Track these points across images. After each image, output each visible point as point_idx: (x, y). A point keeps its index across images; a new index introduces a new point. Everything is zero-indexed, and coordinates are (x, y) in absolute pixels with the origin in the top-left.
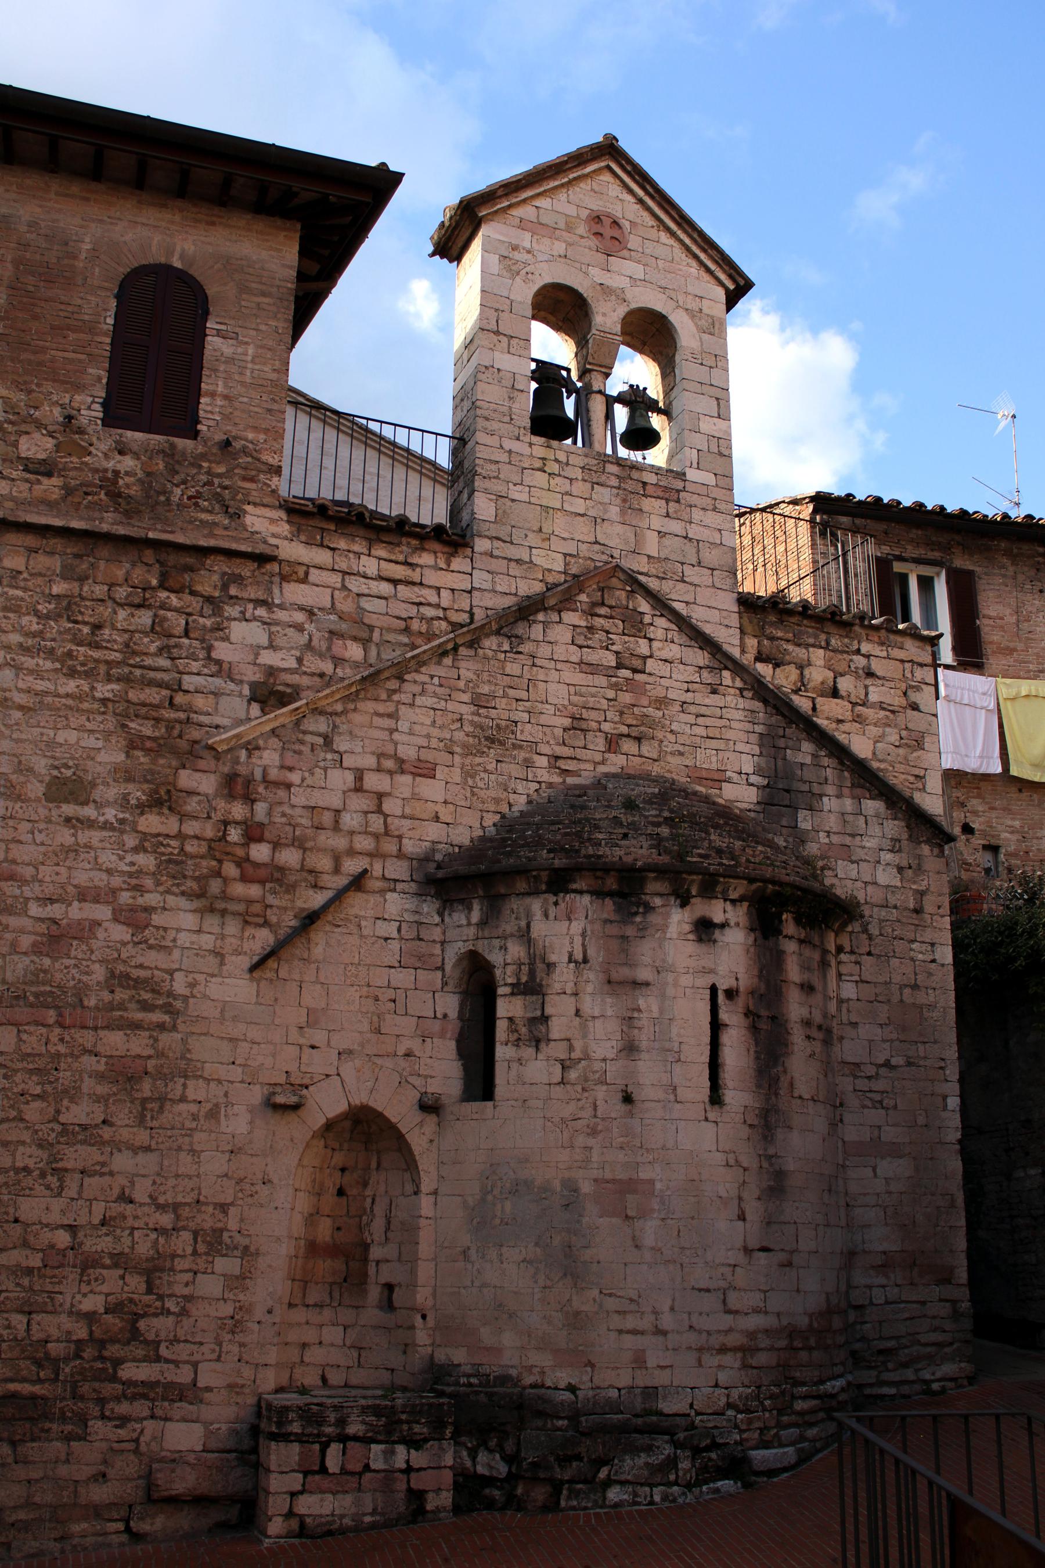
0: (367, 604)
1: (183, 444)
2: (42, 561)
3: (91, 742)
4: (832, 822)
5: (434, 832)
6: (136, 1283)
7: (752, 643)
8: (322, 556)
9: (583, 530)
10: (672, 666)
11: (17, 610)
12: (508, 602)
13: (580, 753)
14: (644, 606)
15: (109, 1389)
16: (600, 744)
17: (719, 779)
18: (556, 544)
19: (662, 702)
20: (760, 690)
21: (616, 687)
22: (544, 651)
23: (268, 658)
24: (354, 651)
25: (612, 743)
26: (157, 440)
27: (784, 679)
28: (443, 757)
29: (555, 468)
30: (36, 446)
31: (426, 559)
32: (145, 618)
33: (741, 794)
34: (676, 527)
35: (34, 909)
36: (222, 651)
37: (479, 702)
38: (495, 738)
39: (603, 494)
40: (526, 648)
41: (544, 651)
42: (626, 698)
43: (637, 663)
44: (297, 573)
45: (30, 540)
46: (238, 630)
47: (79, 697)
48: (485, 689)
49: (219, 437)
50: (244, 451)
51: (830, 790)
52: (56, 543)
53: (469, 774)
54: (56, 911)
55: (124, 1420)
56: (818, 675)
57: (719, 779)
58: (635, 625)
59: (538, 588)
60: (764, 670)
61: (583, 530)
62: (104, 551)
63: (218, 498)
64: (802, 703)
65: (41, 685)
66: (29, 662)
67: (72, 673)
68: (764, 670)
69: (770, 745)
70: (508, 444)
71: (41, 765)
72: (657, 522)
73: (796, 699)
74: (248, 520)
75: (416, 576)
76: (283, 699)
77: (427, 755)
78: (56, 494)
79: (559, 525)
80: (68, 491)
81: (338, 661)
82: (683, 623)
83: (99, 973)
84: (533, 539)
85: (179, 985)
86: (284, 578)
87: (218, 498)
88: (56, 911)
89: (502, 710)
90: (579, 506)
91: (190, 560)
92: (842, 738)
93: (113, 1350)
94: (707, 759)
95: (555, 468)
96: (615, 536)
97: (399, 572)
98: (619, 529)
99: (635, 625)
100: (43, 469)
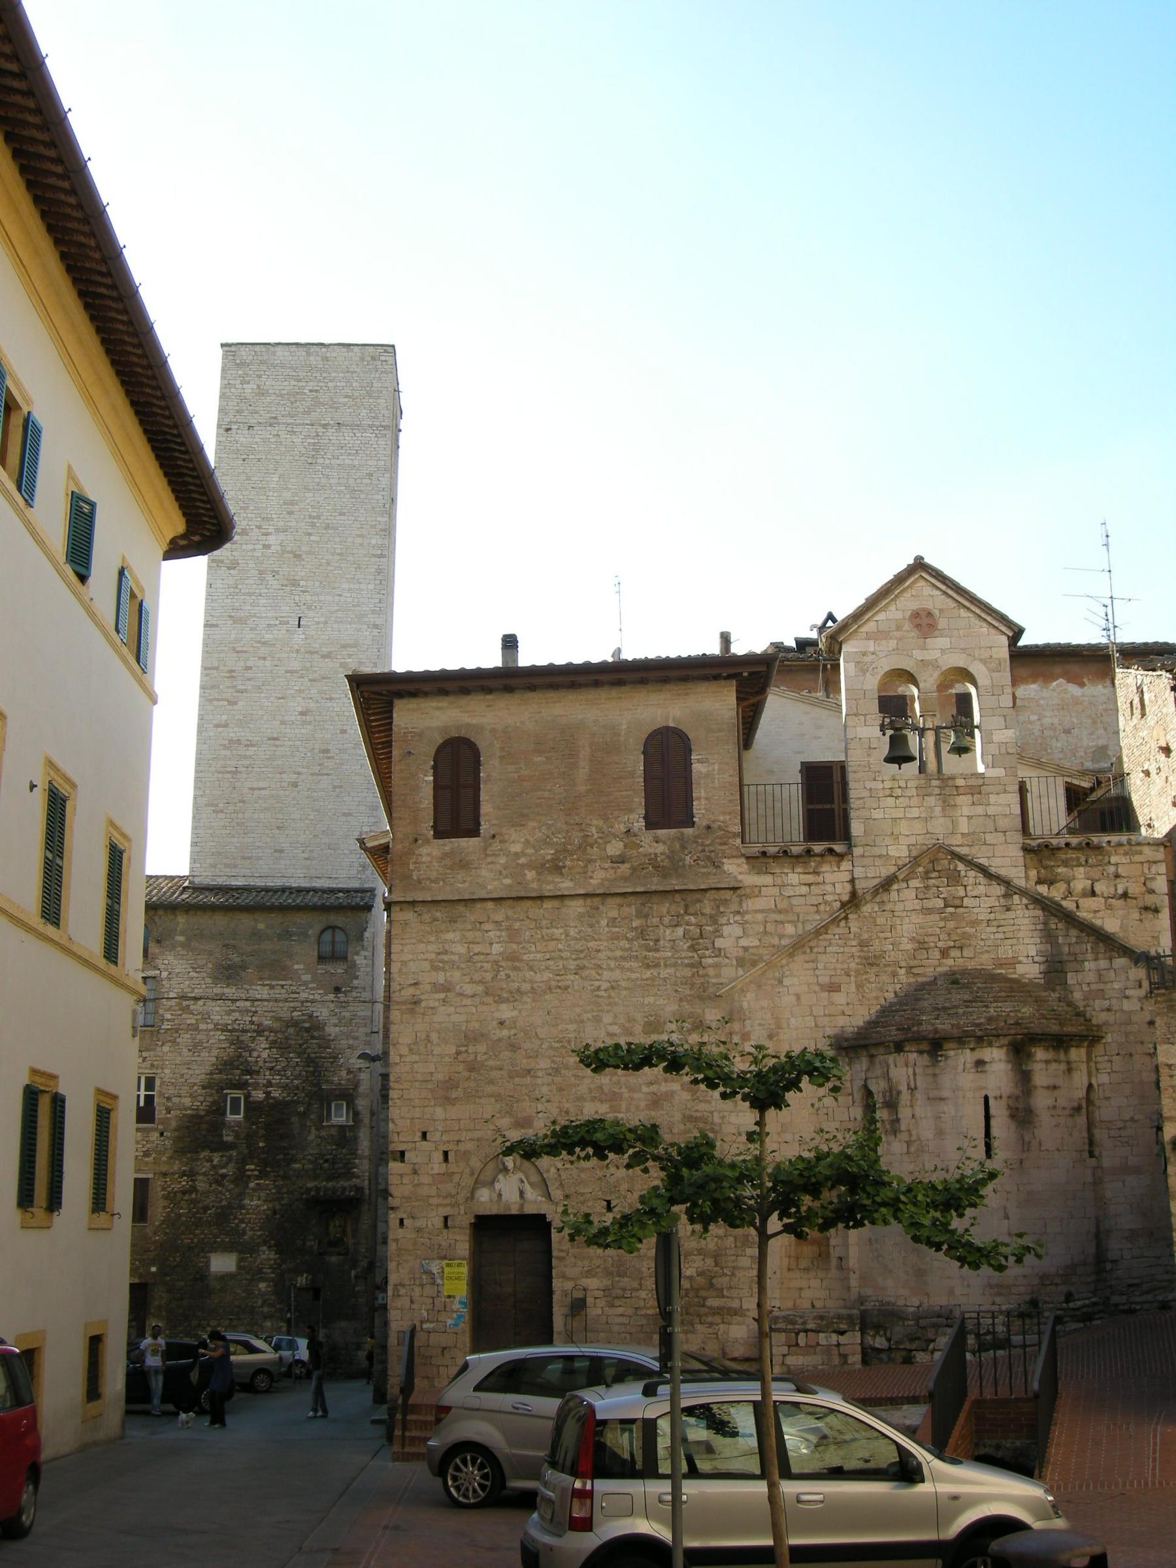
0: (794, 901)
1: (689, 831)
2: (626, 910)
3: (661, 1002)
4: (1091, 977)
5: (841, 1021)
6: (710, 1262)
7: (1033, 873)
8: (767, 879)
9: (919, 827)
10: (981, 899)
11: (617, 938)
12: (876, 882)
13: (925, 962)
14: (961, 867)
15: (703, 1310)
16: (937, 955)
17: (1013, 962)
18: (902, 840)
19: (975, 923)
20: (1038, 901)
21: (945, 919)
22: (899, 907)
23: (744, 942)
24: (790, 929)
25: (944, 953)
26: (673, 832)
27: (1056, 893)
28: (845, 979)
29: (899, 792)
30: (615, 848)
31: (825, 868)
32: (680, 931)
33: (1030, 970)
34: (980, 810)
35: (645, 1089)
36: (719, 943)
37: (863, 944)
38: (871, 962)
39: (931, 801)
40: (889, 907)
41: (899, 907)
42: (951, 924)
43: (957, 902)
44: (757, 891)
45: (619, 900)
46: (726, 930)
47: (653, 979)
48: (865, 936)
49: (705, 823)
50: (720, 828)
51: (1089, 956)
52: (631, 899)
53: (859, 986)
54: (654, 1088)
55: (711, 1324)
56: (1080, 884)
57: (1013, 962)
58: (954, 878)
59: (893, 869)
60: (1043, 889)
61: (919, 827)
62: (655, 899)
63: (709, 858)
64: (1069, 905)
65: (634, 976)
66: (627, 965)
67: (648, 967)
68: (1043, 889)
69: (1048, 936)
70: (869, 785)
71: (639, 1016)
72: (966, 811)
73: (1064, 903)
74: (726, 867)
75: (820, 879)
76: (754, 964)
77: (835, 980)
78: (628, 872)
79: (903, 828)
80: (634, 869)
81: (781, 937)
82: (984, 870)
83: (678, 1116)
84: (888, 841)
85: (717, 1120)
86: (748, 896)
87: (709, 858)
88: (654, 1088)
89: (876, 946)
90: (915, 812)
91: (698, 896)
92: (1098, 922)
93: (703, 1293)
94: (1006, 952)
95: (899, 792)
96: (939, 827)
97: (810, 878)
98: (942, 820)
99: (954, 878)
100: (621, 859)
